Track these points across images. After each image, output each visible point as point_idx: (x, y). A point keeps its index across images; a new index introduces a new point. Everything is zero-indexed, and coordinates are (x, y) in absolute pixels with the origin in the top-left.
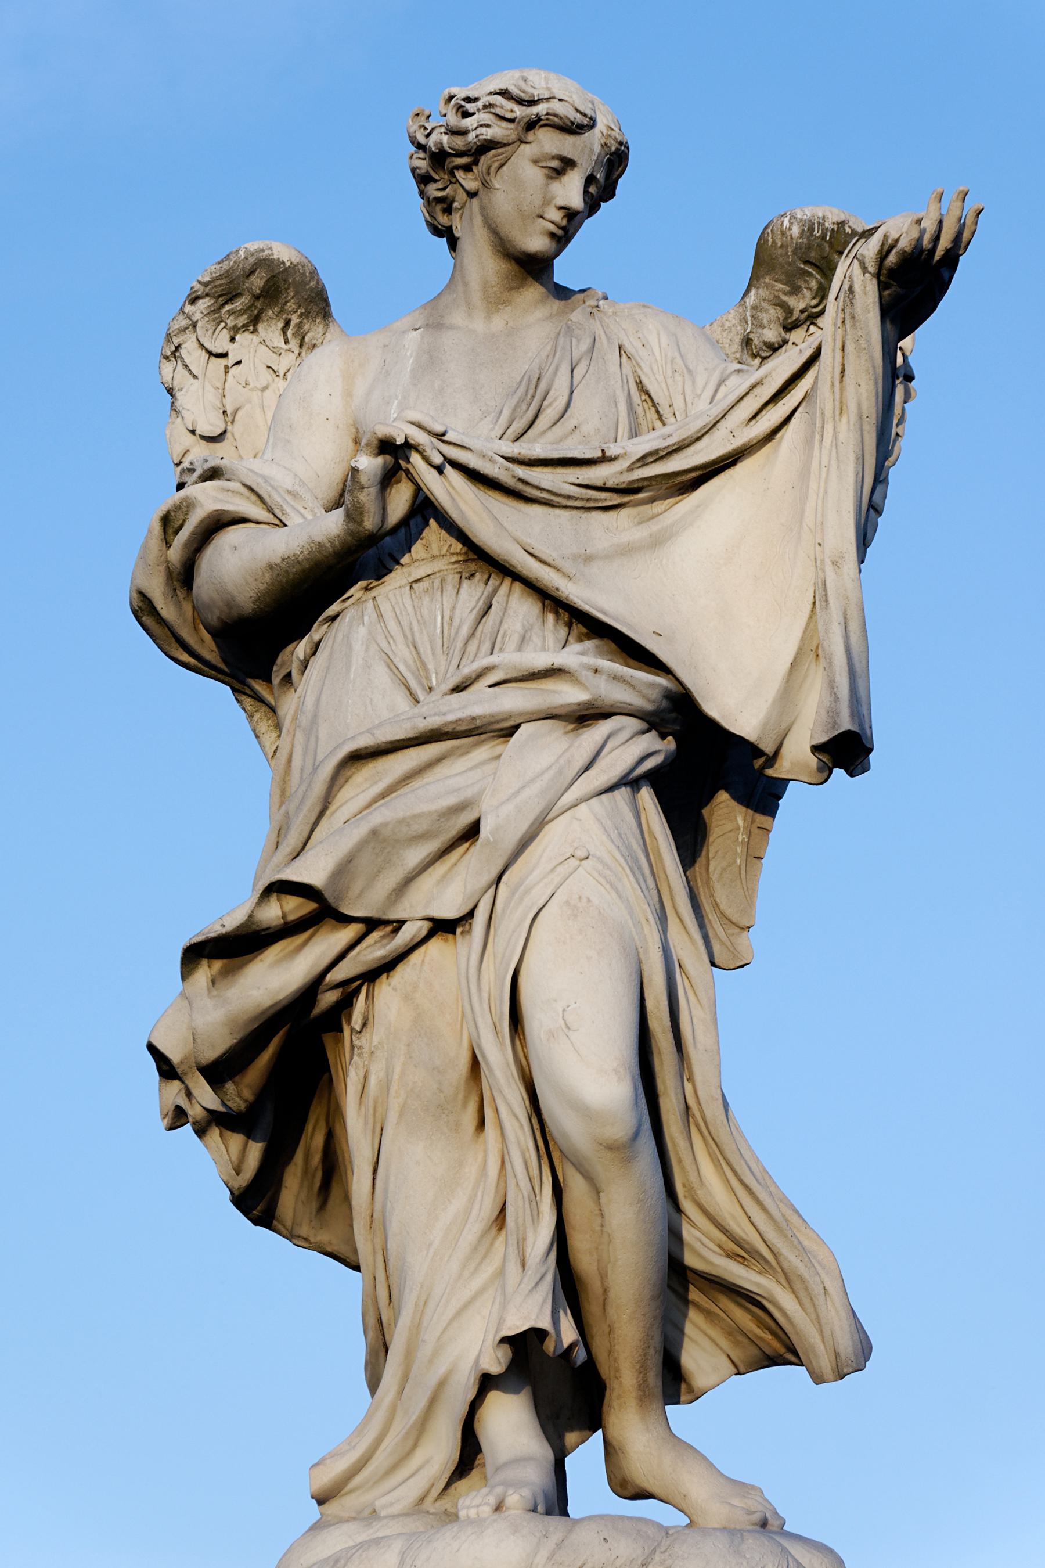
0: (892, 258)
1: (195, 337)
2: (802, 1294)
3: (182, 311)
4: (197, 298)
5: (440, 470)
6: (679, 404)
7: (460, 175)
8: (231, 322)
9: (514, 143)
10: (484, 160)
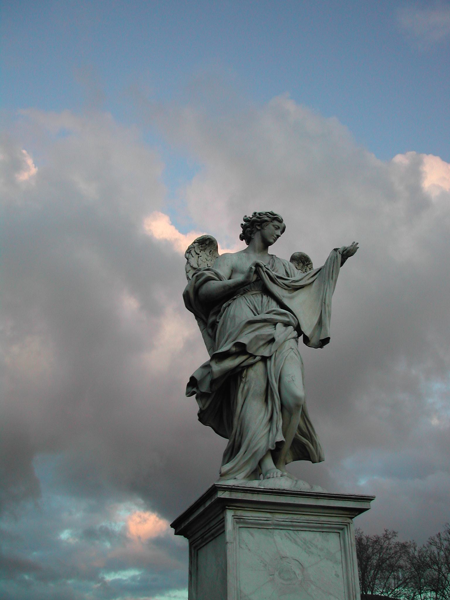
0: (345, 252)
1: (194, 250)
2: (314, 444)
3: (192, 244)
4: (196, 243)
6: (293, 275)
8: (201, 248)
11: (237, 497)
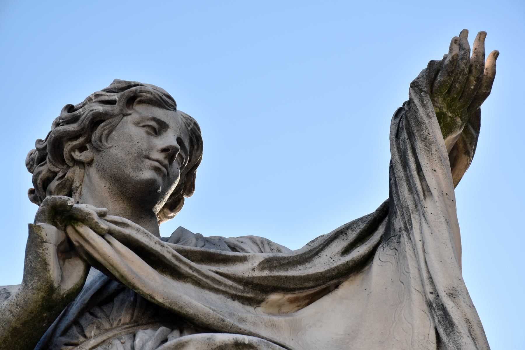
7: (77, 155)
9: (118, 115)
10: (95, 137)
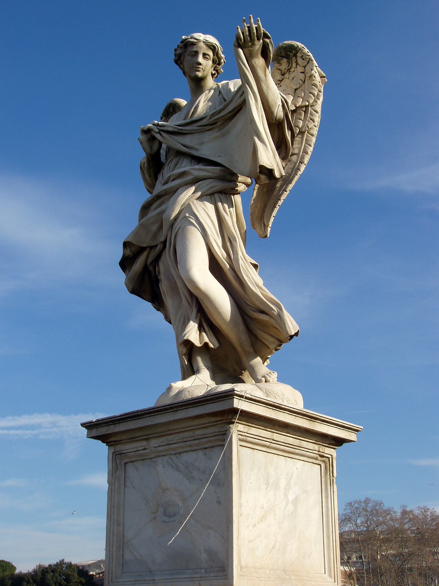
5: (159, 133)
11: (102, 433)
